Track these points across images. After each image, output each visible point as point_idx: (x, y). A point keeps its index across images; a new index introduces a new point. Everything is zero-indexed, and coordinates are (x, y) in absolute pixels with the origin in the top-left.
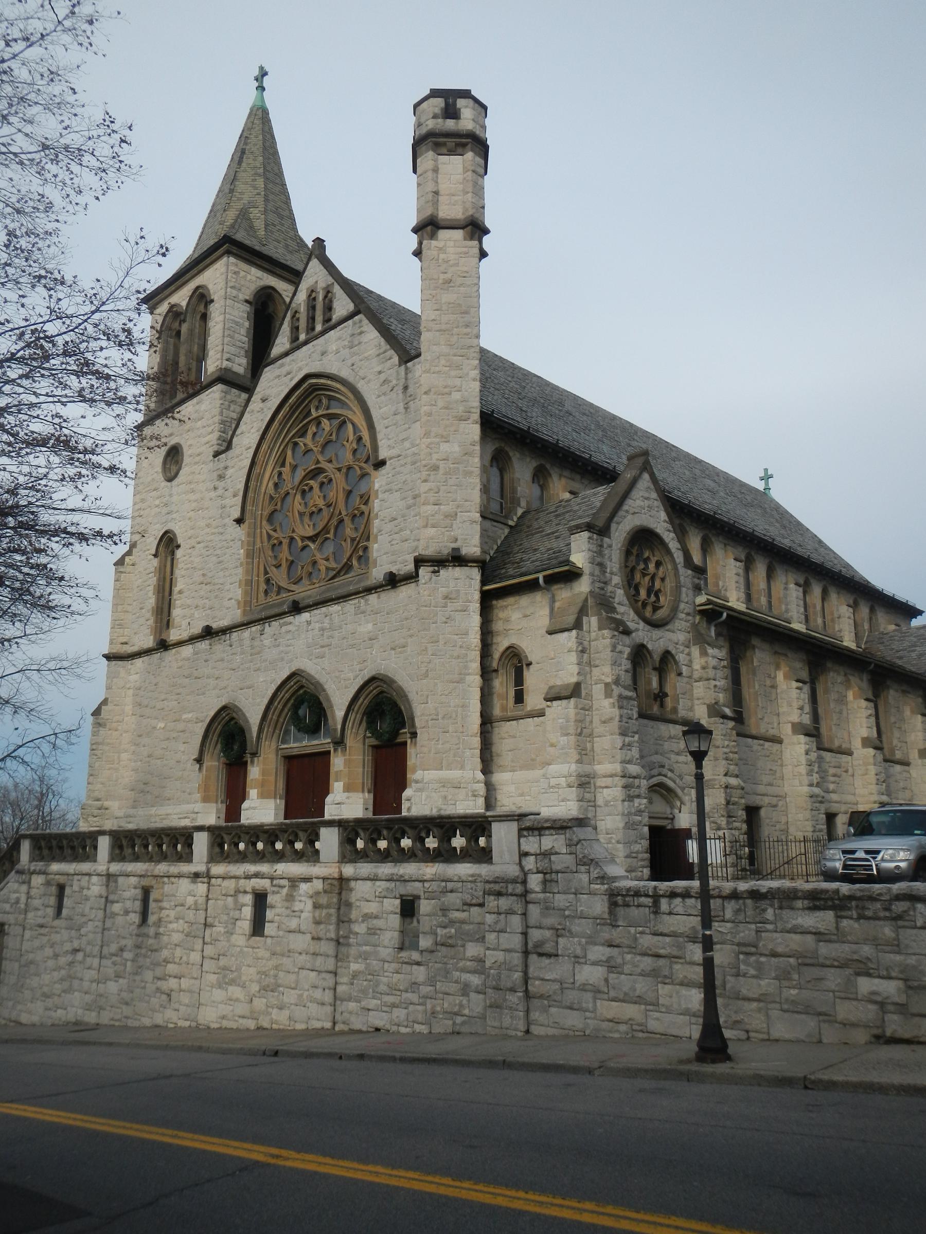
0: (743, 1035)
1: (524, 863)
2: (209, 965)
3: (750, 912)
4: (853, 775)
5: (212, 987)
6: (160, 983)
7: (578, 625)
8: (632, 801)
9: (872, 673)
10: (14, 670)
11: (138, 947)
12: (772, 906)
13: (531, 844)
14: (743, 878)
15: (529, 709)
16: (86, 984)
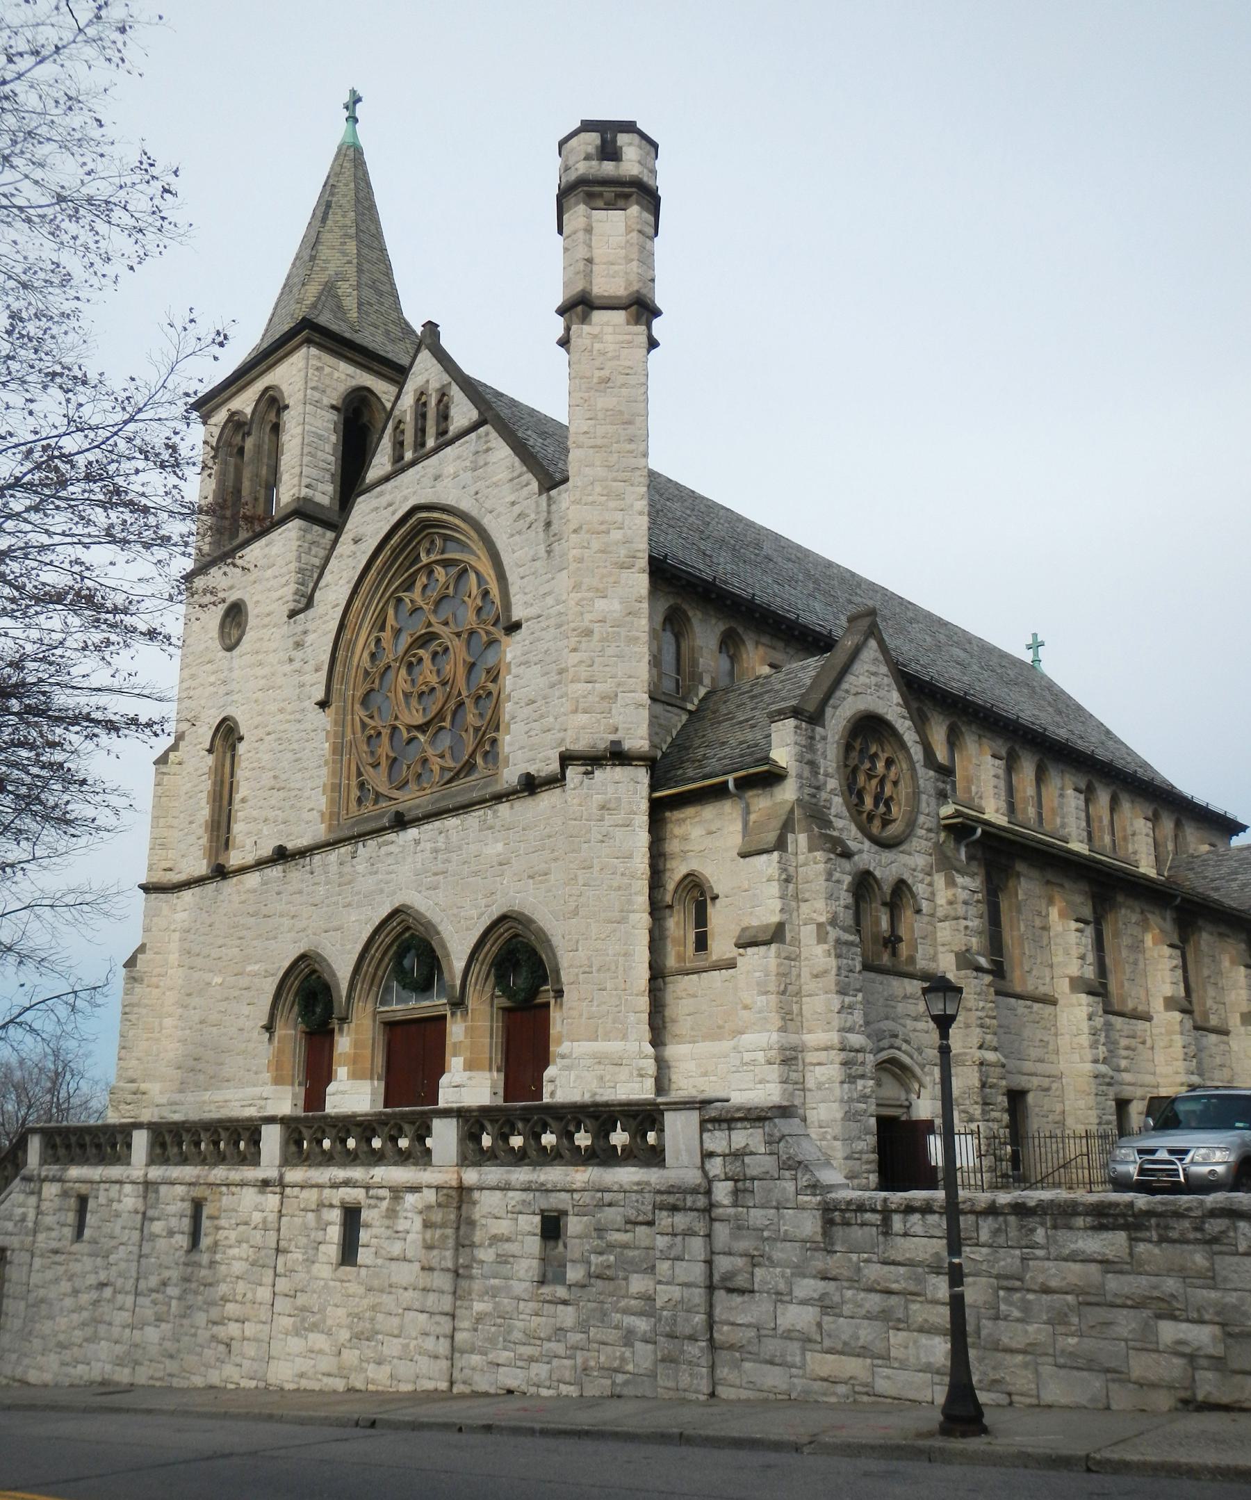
0: (1003, 1400)
1: (708, 1166)
2: (282, 1305)
3: (1013, 1233)
4: (1152, 1048)
5: (286, 1334)
6: (216, 1329)
7: (780, 845)
8: (854, 1083)
9: (1178, 909)
10: (19, 905)
11: (187, 1280)
12: (1043, 1224)
13: (717, 1141)
14: (1005, 1187)
15: (714, 958)
16: (116, 1331)
